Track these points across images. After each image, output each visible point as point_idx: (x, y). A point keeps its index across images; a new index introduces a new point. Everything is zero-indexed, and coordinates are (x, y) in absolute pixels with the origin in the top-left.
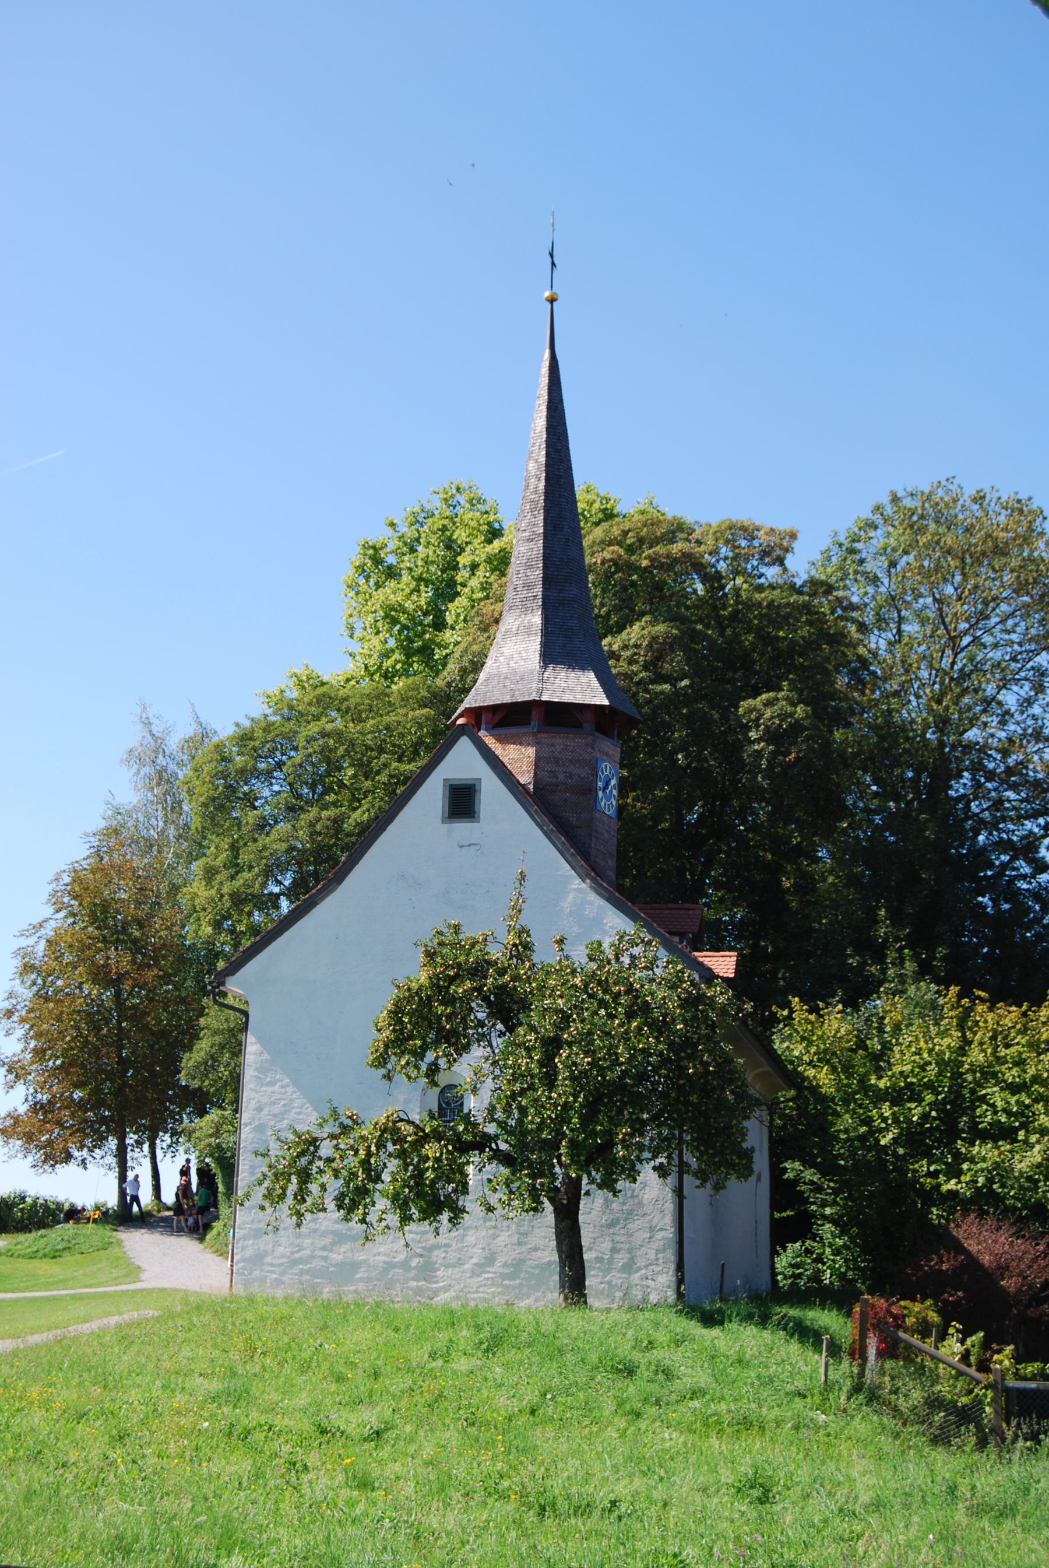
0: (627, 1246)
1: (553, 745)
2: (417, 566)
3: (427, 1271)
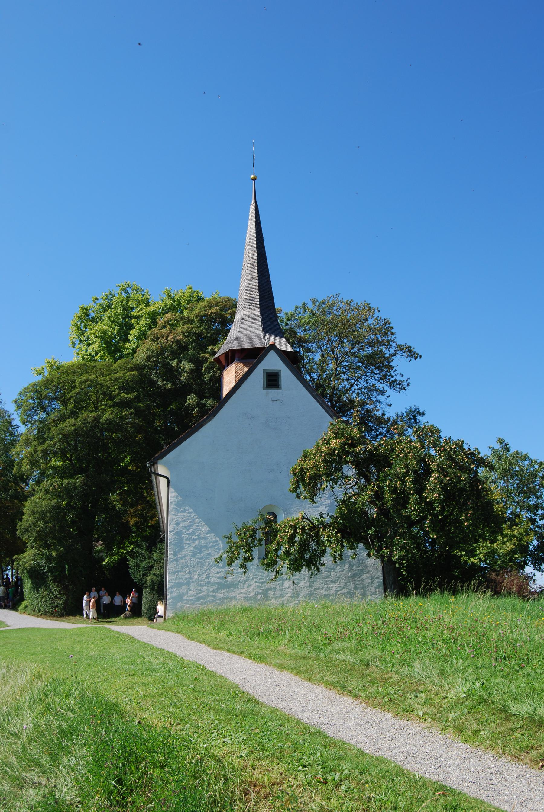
0: (361, 586)
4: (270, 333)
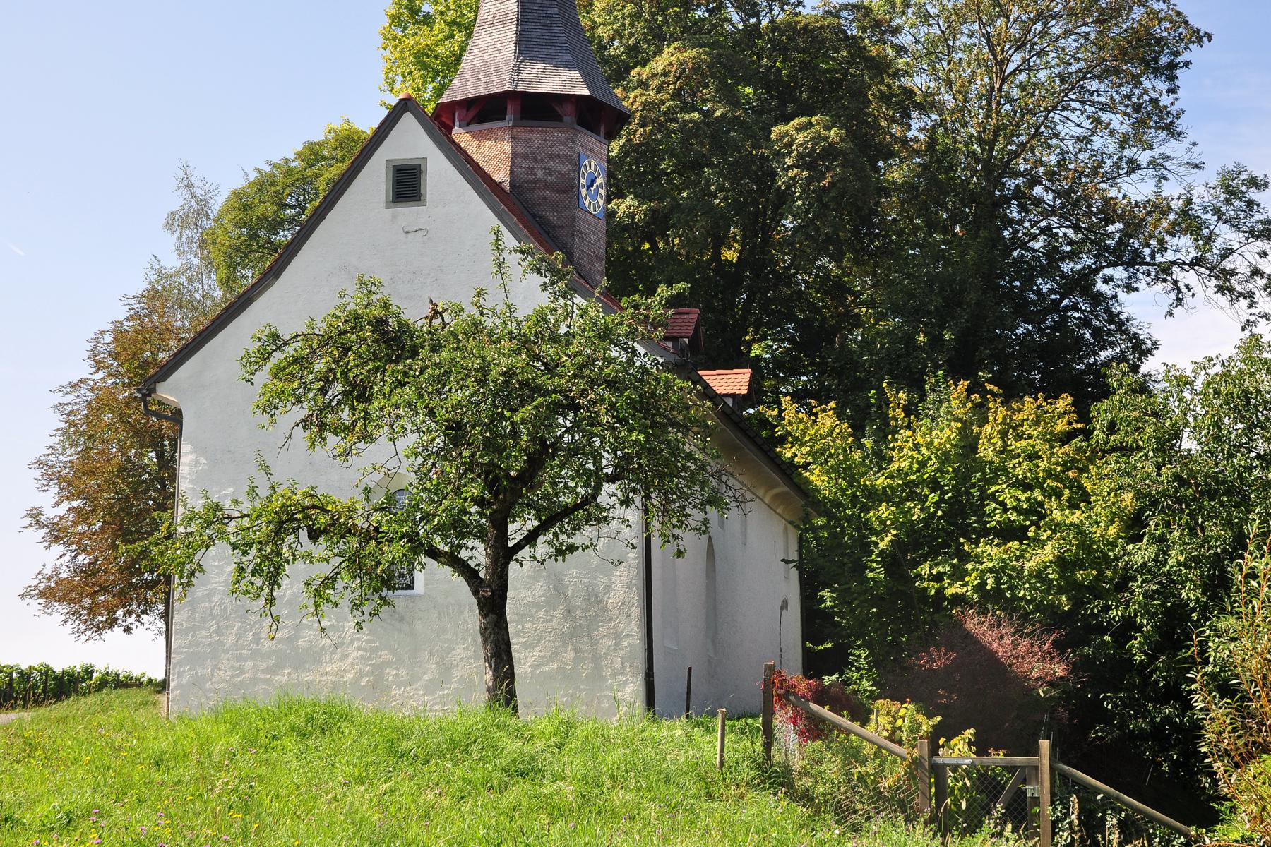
1: (530, 140)
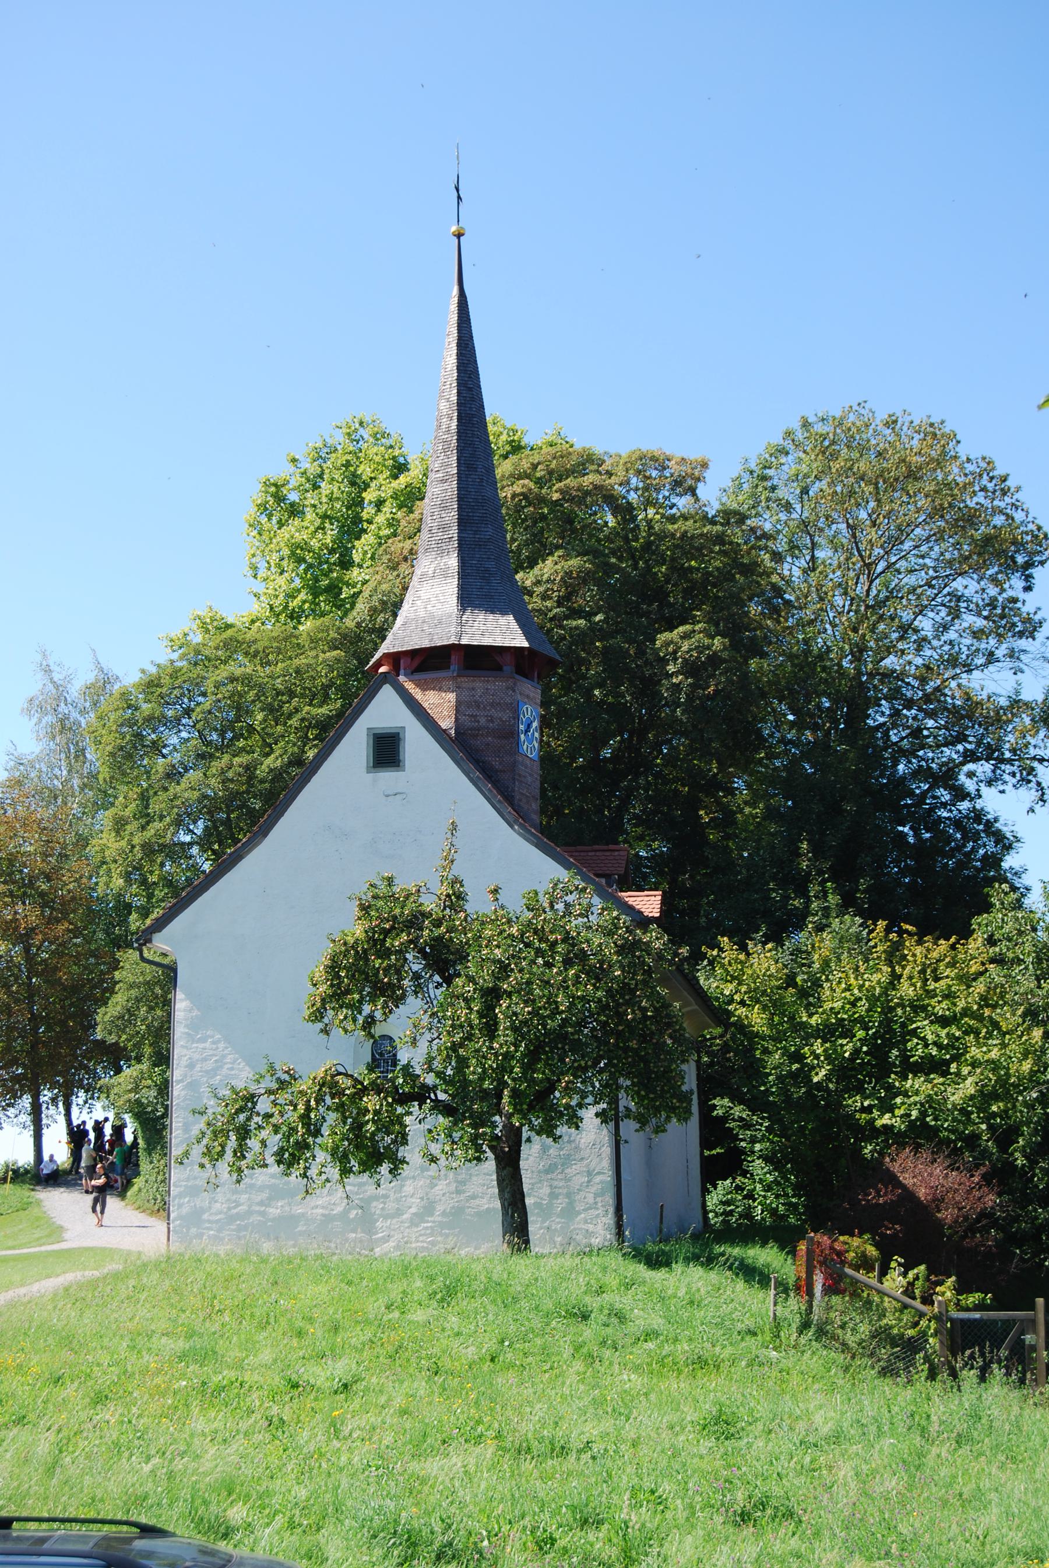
0: (565, 1191)
1: (473, 689)
2: (321, 503)
3: (367, 1222)
4: (475, 606)
